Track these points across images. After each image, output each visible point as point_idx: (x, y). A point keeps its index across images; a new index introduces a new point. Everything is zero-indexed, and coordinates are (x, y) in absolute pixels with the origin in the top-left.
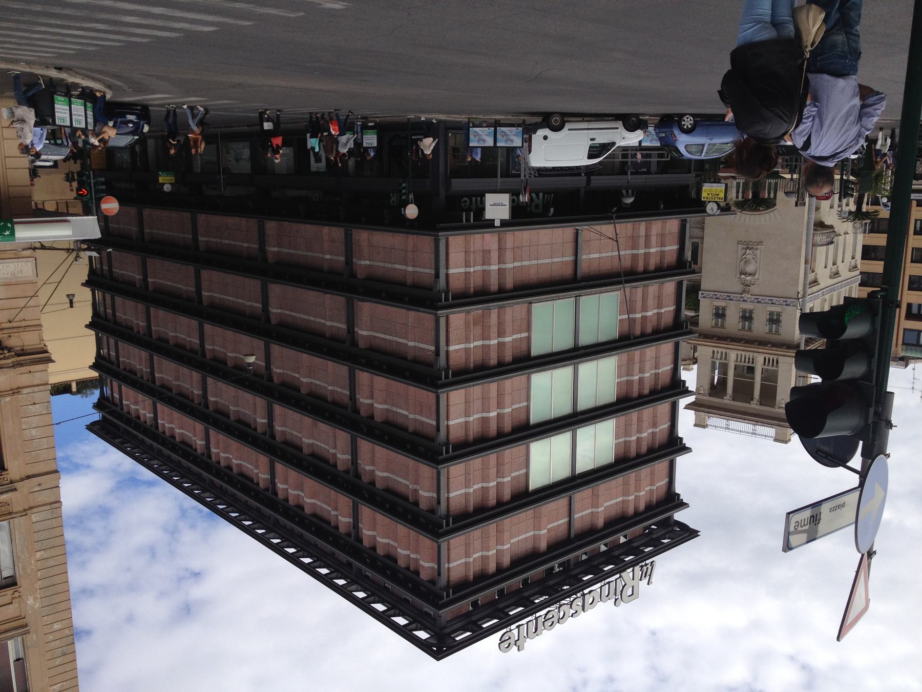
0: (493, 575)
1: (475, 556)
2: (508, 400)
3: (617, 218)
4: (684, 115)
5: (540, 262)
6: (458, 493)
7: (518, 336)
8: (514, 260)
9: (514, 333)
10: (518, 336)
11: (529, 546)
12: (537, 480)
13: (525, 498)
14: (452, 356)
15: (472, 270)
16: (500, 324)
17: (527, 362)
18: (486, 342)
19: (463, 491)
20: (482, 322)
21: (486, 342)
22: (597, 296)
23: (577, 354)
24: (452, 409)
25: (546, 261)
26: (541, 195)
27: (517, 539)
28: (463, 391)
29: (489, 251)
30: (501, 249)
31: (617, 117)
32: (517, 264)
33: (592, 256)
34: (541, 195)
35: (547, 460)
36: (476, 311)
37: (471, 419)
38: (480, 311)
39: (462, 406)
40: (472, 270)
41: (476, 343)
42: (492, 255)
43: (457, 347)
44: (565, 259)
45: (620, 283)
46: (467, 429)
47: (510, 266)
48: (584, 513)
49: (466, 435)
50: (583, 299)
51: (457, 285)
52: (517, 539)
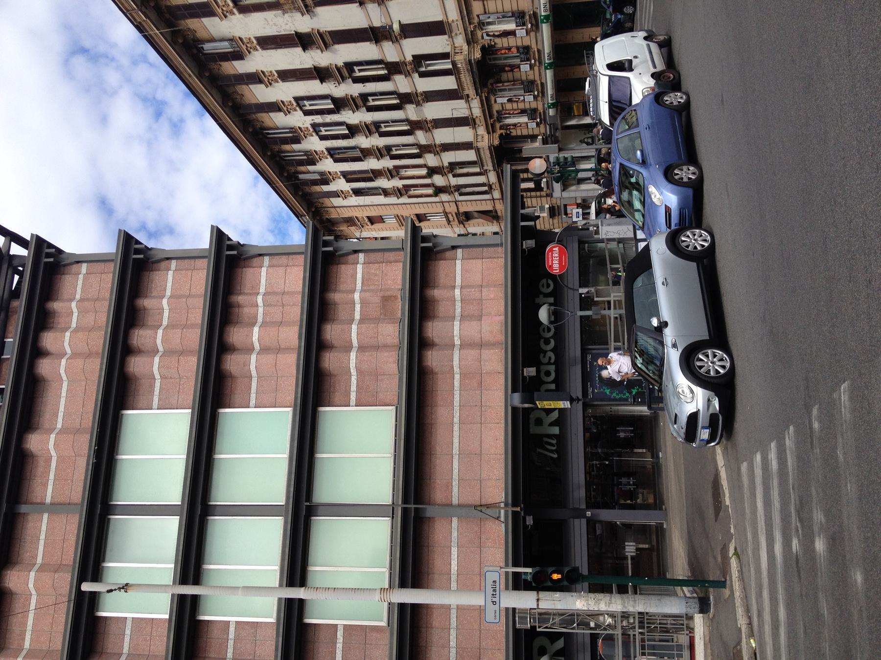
0: (36, 339)
1: (75, 315)
2: (269, 358)
3: (514, 513)
4: (685, 93)
5: (456, 428)
6: (169, 285)
7: (354, 388)
8: (463, 376)
9: (360, 372)
10: (354, 388)
11: (45, 418)
12: (135, 419)
13: (118, 392)
14: (351, 266)
15: (457, 292)
16: (377, 348)
17: (314, 392)
18: (356, 322)
19: (168, 293)
20: (386, 314)
21: (356, 322)
22: (388, 565)
23: (302, 510)
24: (281, 270)
25: (456, 441)
26: (556, 430)
27: (64, 394)
28: (299, 288)
29: (480, 320)
30: (481, 345)
31: (670, 61)
32: (457, 384)
33: (454, 551)
34: (556, 430)
35: (156, 446)
36: (400, 308)
37: (260, 299)
38: (399, 315)
39: (280, 288)
40: (457, 292)
41: (358, 307)
42: (474, 324)
43: (359, 276)
44: (455, 490)
45: (405, 500)
46: (247, 294)
47: (456, 362)
48: (42, 543)
49: (240, 294)
50: (388, 520)
51: (441, 268)
52: (64, 394)
